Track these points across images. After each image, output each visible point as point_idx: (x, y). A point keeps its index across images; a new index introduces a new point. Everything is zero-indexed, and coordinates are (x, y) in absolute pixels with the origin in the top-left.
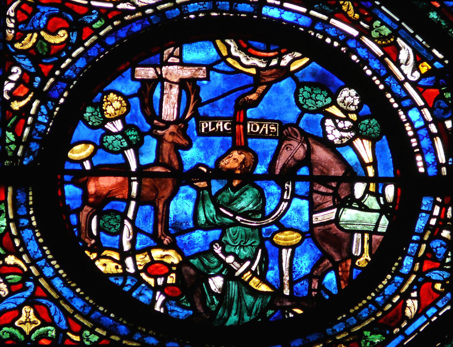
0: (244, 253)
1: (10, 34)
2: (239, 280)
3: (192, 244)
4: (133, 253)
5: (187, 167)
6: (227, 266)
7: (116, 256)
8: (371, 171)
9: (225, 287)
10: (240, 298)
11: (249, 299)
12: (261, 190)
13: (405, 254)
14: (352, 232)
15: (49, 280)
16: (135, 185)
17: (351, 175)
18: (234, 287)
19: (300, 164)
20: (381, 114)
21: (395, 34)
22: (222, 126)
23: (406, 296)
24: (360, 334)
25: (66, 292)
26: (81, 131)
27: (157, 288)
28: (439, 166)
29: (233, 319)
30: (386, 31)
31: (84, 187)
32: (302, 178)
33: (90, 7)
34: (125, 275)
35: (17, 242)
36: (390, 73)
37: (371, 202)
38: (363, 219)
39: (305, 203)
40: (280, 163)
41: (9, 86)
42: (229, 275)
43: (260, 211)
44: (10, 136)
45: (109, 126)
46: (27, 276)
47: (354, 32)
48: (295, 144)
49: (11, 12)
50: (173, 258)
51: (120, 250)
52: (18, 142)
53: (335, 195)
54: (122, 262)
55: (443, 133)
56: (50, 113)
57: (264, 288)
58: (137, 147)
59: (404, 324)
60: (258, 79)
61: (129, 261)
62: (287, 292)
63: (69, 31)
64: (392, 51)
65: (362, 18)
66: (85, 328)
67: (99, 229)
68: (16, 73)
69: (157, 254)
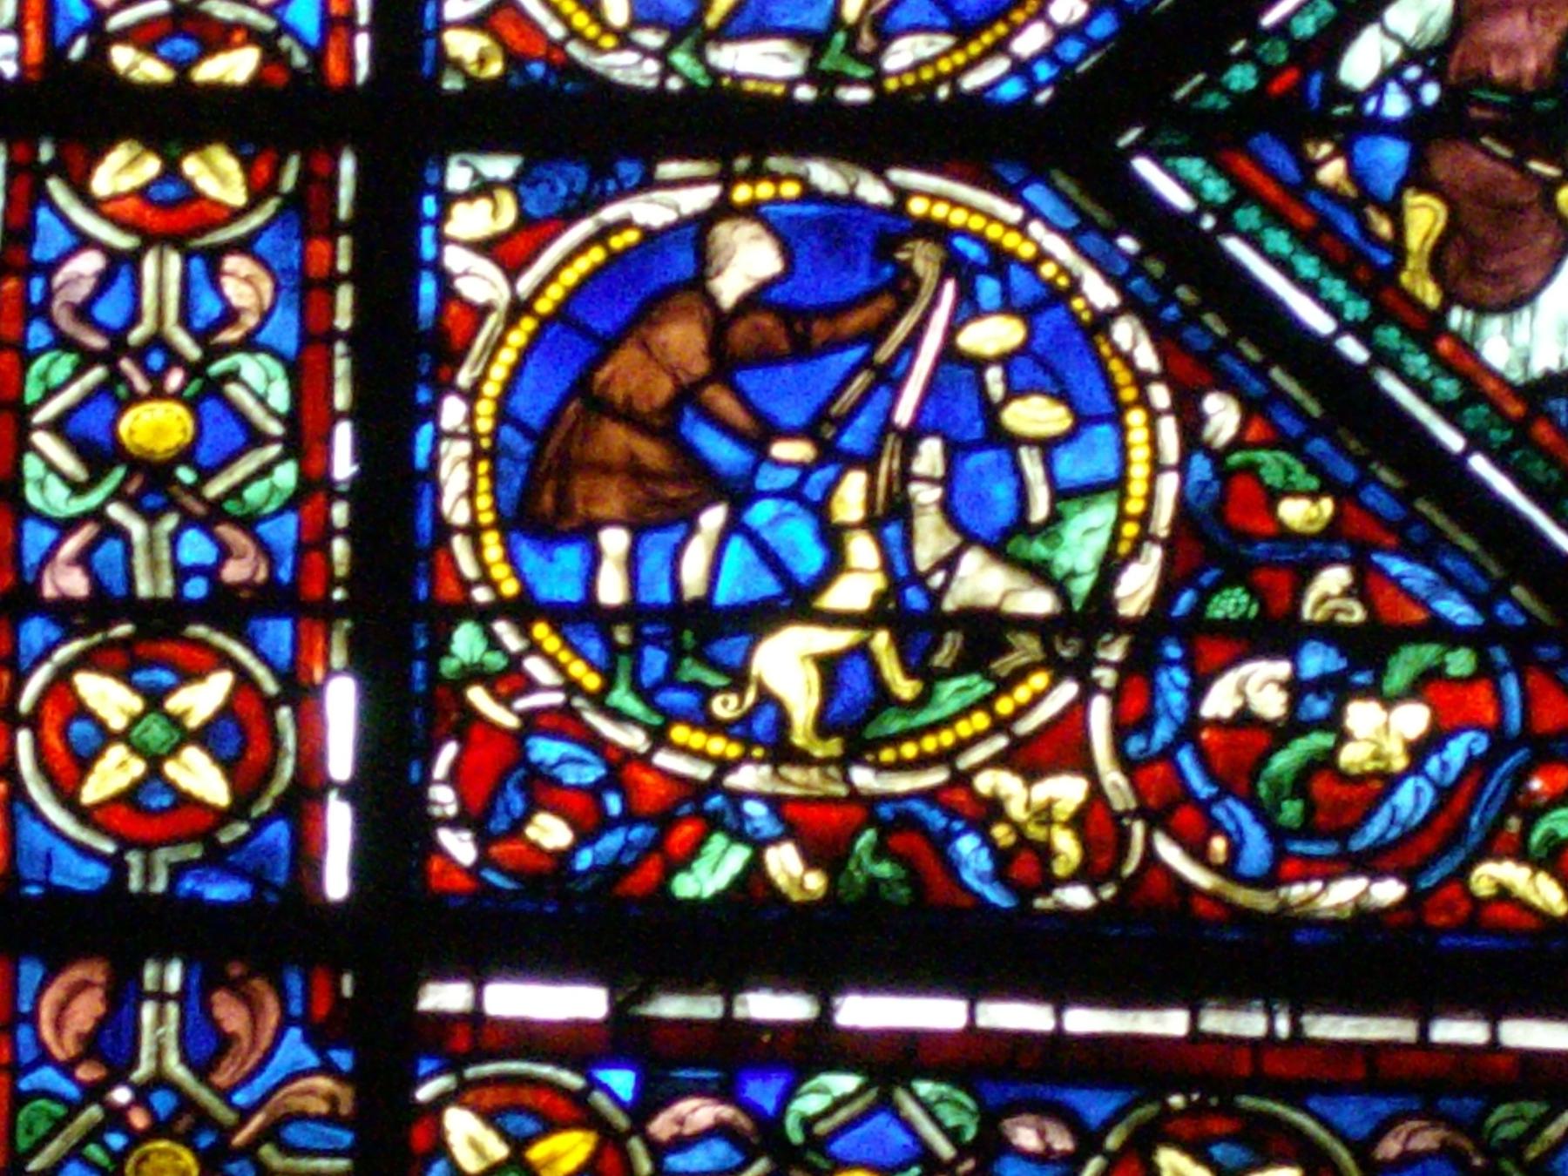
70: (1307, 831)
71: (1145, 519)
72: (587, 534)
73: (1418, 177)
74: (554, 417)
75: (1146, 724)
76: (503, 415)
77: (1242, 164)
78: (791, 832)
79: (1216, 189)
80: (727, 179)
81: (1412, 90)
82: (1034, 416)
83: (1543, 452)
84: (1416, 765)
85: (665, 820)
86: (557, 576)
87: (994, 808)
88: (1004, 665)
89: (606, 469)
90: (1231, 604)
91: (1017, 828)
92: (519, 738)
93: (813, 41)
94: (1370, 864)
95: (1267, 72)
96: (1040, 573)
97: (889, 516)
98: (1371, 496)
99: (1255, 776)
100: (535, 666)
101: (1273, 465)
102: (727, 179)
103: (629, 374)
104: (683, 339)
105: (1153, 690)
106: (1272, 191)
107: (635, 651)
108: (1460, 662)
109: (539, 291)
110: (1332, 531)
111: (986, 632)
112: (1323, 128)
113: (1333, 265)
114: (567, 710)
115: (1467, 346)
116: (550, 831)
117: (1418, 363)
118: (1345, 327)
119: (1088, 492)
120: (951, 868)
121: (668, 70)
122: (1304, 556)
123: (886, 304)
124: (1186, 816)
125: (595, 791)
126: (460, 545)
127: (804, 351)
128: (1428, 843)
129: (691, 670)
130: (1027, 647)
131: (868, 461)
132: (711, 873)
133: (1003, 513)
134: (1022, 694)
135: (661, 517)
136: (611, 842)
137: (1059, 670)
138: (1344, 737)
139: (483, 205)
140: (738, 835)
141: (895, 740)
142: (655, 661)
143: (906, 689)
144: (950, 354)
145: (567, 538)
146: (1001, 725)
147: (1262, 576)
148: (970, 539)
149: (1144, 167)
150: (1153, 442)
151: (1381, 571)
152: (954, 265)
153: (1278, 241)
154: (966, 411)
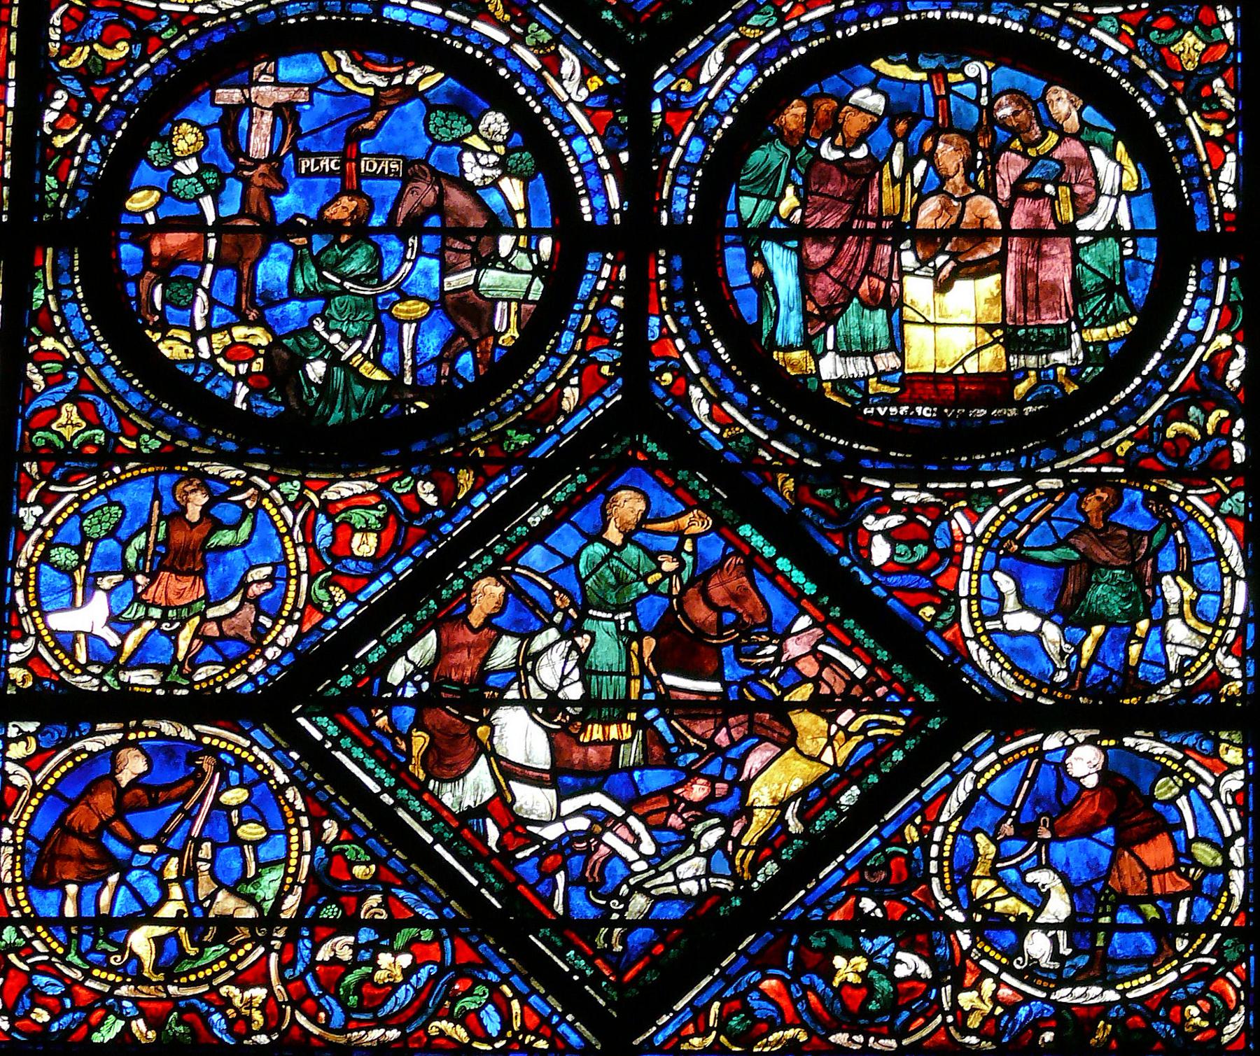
0: (354, 330)
1: (54, 48)
2: (346, 365)
3: (286, 318)
4: (208, 332)
5: (281, 219)
6: (331, 347)
7: (186, 337)
8: (521, 221)
9: (328, 376)
10: (347, 388)
11: (359, 390)
12: (377, 247)
13: (563, 329)
14: (495, 301)
15: (97, 369)
16: (212, 243)
17: (496, 225)
18: (339, 374)
19: (428, 212)
20: (536, 147)
21: (557, 40)
22: (329, 164)
23: (564, 383)
24: (502, 435)
25: (120, 385)
26: (144, 173)
27: (239, 377)
28: (611, 212)
29: (337, 416)
30: (546, 37)
31: (146, 247)
32: (432, 231)
33: (159, 11)
34: (197, 361)
35: (57, 321)
36: (549, 92)
37: (521, 260)
38: (510, 283)
39: (434, 263)
40: (403, 212)
41: (50, 117)
42: (334, 358)
43: (375, 275)
44: (51, 182)
45: (179, 166)
46: (69, 364)
47: (503, 38)
48: (422, 186)
49: (55, 19)
50: (261, 338)
51: (191, 329)
52: (61, 189)
53: (474, 253)
54: (193, 344)
55: (616, 168)
56: (104, 150)
57: (379, 375)
58: (216, 193)
59: (561, 420)
60: (376, 102)
61: (202, 343)
62: (408, 380)
63: (131, 42)
64: (552, 62)
65: (514, 20)
66: (143, 431)
67: (164, 301)
68: (60, 99)
69: (239, 332)
70: (360, 1009)
71: (295, 875)
72: (61, 887)
73: (418, 724)
74: (49, 835)
75: (293, 964)
76: (26, 836)
77: (344, 720)
78: (142, 1014)
79: (333, 730)
80: (126, 730)
81: (417, 685)
82: (252, 831)
83: (467, 843)
84: (406, 980)
85: (89, 1010)
86: (47, 905)
87: (228, 1001)
88: (233, 940)
89: (70, 858)
90: (331, 912)
91: (237, 1010)
92: (29, 975)
93: (164, 669)
94: (385, 1023)
95: (357, 679)
96: (251, 900)
97: (188, 875)
98: (393, 863)
99: (338, 986)
100: (37, 944)
101: (351, 850)
102: (126, 730)
103: (81, 817)
104: (104, 801)
105: (296, 949)
106: (355, 730)
107: (79, 937)
108: (427, 935)
109: (45, 781)
110: (375, 878)
111: (227, 925)
112: (380, 703)
113: (380, 763)
114: (49, 963)
115: (436, 797)
116: (42, 1016)
117: (415, 805)
118: (384, 790)
119: (272, 864)
120: (209, 1027)
121: (103, 683)
122: (362, 890)
123: (190, 783)
124: (309, 1003)
125: (60, 998)
126: (7, 892)
127: (154, 805)
128: (410, 1013)
129: (102, 945)
130: (244, 932)
131: (180, 854)
132: (109, 1031)
133: (236, 875)
134: (241, 952)
135: (91, 878)
136: (66, 1019)
137: (257, 941)
138: (377, 968)
139: (23, 744)
140: (119, 1016)
141: (187, 974)
142: (87, 940)
143: (192, 951)
144: (216, 804)
145: (52, 888)
146: (232, 966)
147: (344, 899)
148: (221, 886)
149: (302, 721)
150: (300, 842)
151: (396, 896)
152: (221, 767)
153: (358, 752)
154: (222, 831)
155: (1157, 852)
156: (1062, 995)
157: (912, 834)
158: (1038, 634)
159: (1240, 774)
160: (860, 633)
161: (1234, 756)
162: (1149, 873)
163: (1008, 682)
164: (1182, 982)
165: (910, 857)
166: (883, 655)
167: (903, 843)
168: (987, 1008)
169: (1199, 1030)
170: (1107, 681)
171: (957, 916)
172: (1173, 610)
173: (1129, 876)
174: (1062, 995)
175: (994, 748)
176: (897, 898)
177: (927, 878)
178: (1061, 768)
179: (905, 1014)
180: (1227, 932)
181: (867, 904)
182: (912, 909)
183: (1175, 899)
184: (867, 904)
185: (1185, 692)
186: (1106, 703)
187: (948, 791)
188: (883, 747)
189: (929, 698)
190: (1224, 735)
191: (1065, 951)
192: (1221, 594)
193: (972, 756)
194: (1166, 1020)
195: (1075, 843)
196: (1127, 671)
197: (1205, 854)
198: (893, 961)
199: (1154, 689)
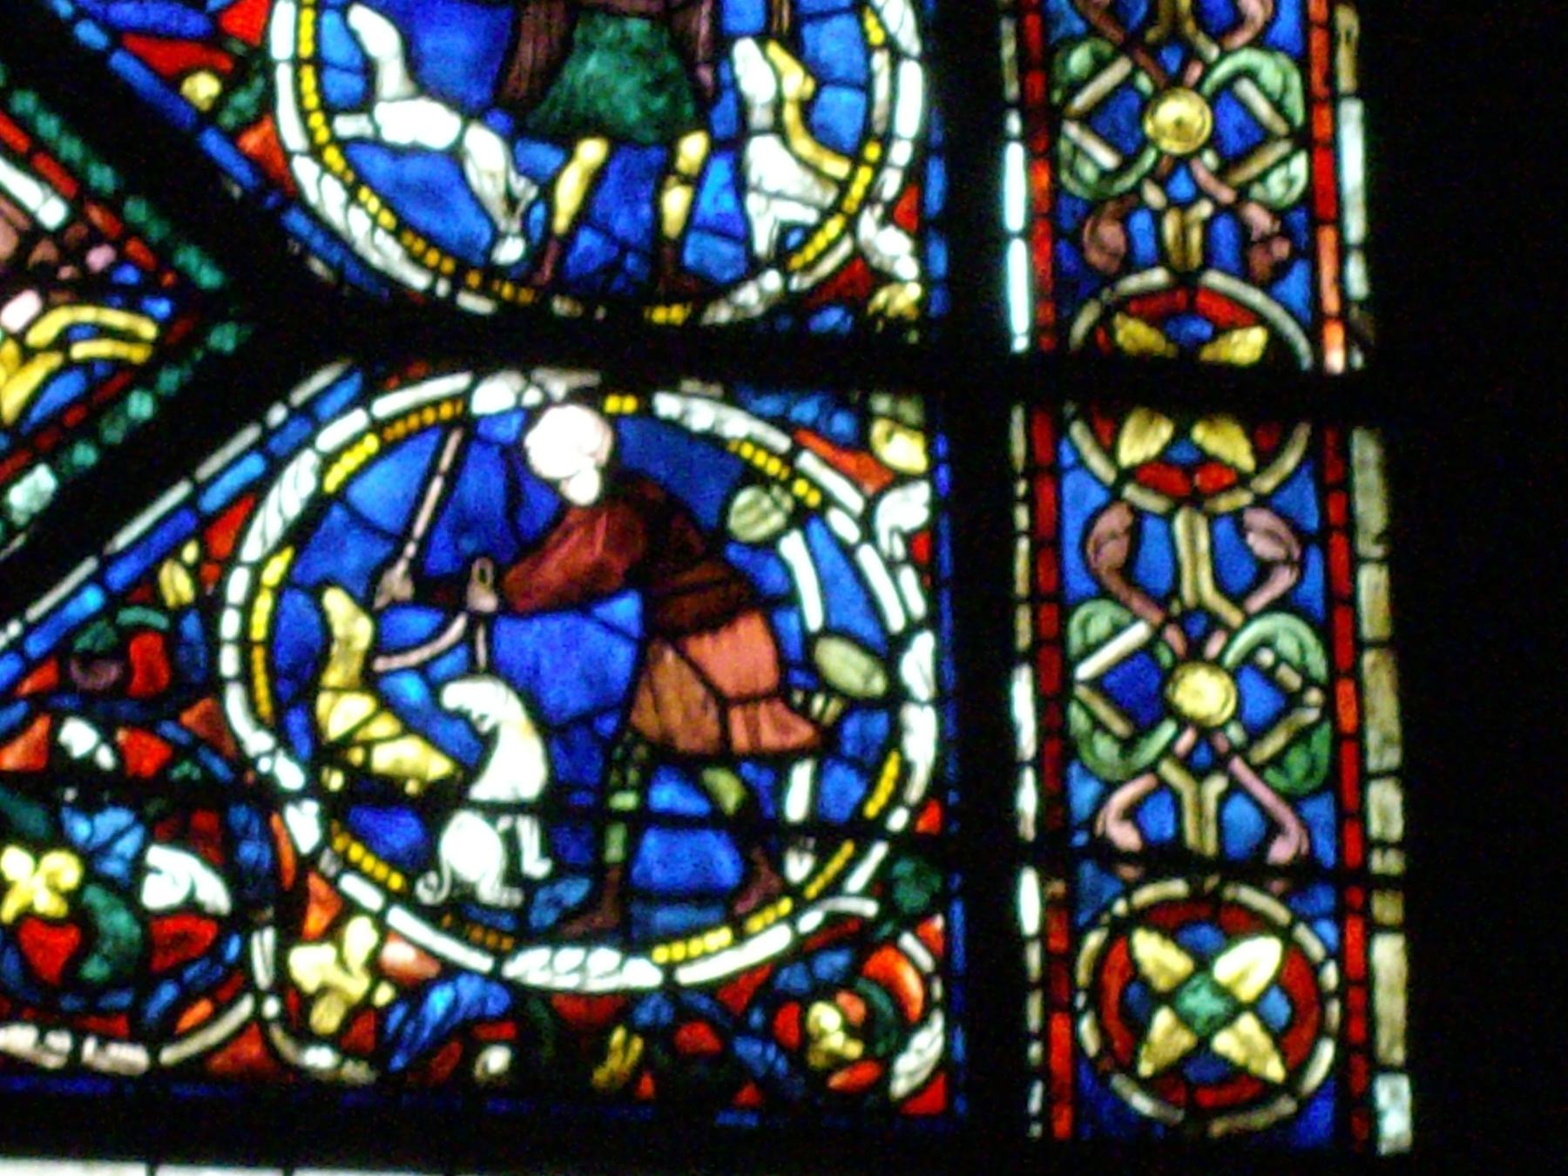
155: (740, 654)
156: (534, 967)
157: (177, 584)
158: (455, 156)
159: (921, 493)
160: (48, 126)
161: (904, 450)
162: (723, 703)
163: (385, 253)
164: (803, 951)
165: (173, 638)
166: (102, 177)
167: (154, 599)
168: (356, 985)
169: (839, 1062)
170: (613, 267)
171: (290, 775)
172: (760, 116)
173: (674, 706)
174: (534, 967)
175: (363, 400)
176: (150, 728)
177: (214, 686)
178: (513, 457)
179: (168, 993)
180: (902, 844)
181: (79, 737)
182: (180, 752)
183: (780, 763)
184: (79, 737)
185: (790, 305)
186: (612, 310)
187: (254, 494)
188: (107, 384)
189: (209, 277)
190: (882, 404)
191: (535, 865)
192: (866, 87)
193: (311, 417)
194: (767, 1035)
195: (555, 626)
196: (660, 251)
197: (845, 665)
198: (138, 868)
199: (722, 290)
